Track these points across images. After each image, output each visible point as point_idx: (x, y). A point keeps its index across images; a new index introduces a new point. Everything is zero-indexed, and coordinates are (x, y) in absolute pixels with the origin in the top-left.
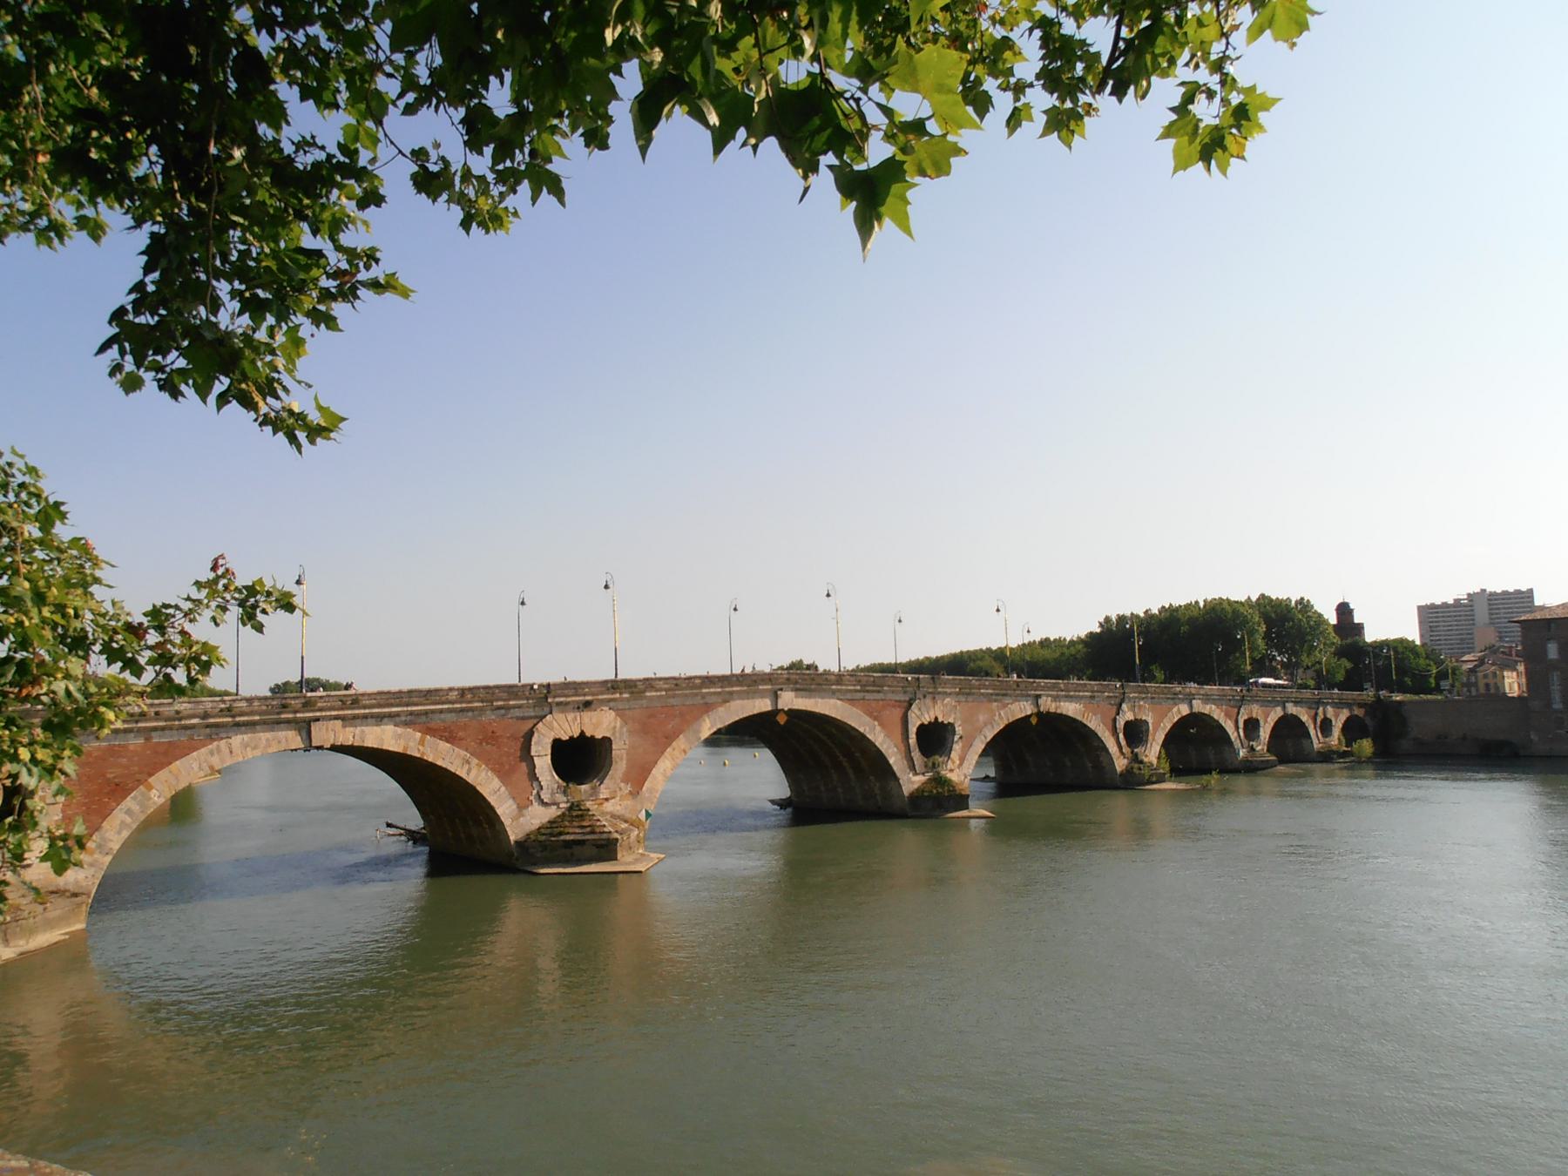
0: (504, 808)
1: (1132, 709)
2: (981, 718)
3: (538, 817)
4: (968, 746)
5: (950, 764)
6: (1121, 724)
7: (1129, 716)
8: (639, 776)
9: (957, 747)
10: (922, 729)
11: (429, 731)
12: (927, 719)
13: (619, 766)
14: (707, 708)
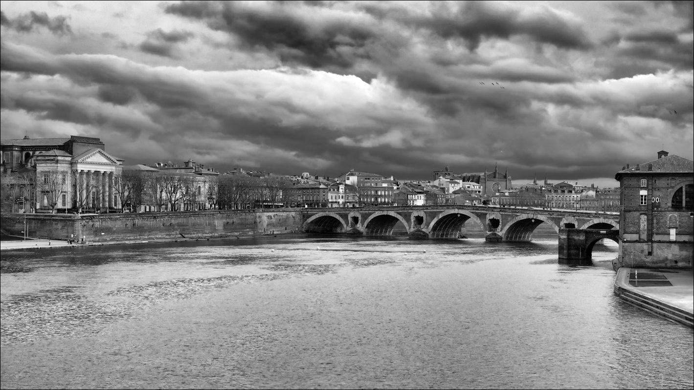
0: (407, 228)
1: (567, 220)
2: (509, 219)
3: (412, 230)
4: (504, 226)
5: (498, 230)
6: (562, 223)
7: (566, 222)
8: (428, 225)
9: (500, 227)
10: (491, 220)
11: (398, 213)
12: (491, 217)
13: (424, 222)
14: (441, 212)
